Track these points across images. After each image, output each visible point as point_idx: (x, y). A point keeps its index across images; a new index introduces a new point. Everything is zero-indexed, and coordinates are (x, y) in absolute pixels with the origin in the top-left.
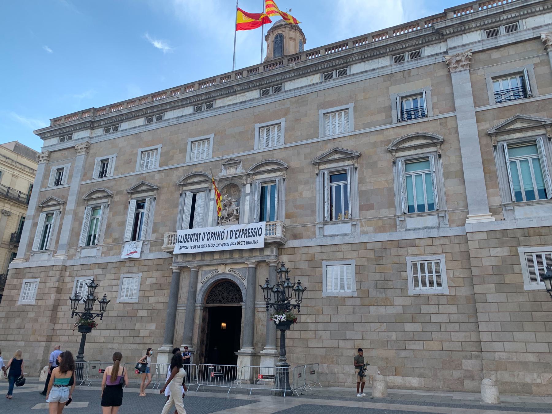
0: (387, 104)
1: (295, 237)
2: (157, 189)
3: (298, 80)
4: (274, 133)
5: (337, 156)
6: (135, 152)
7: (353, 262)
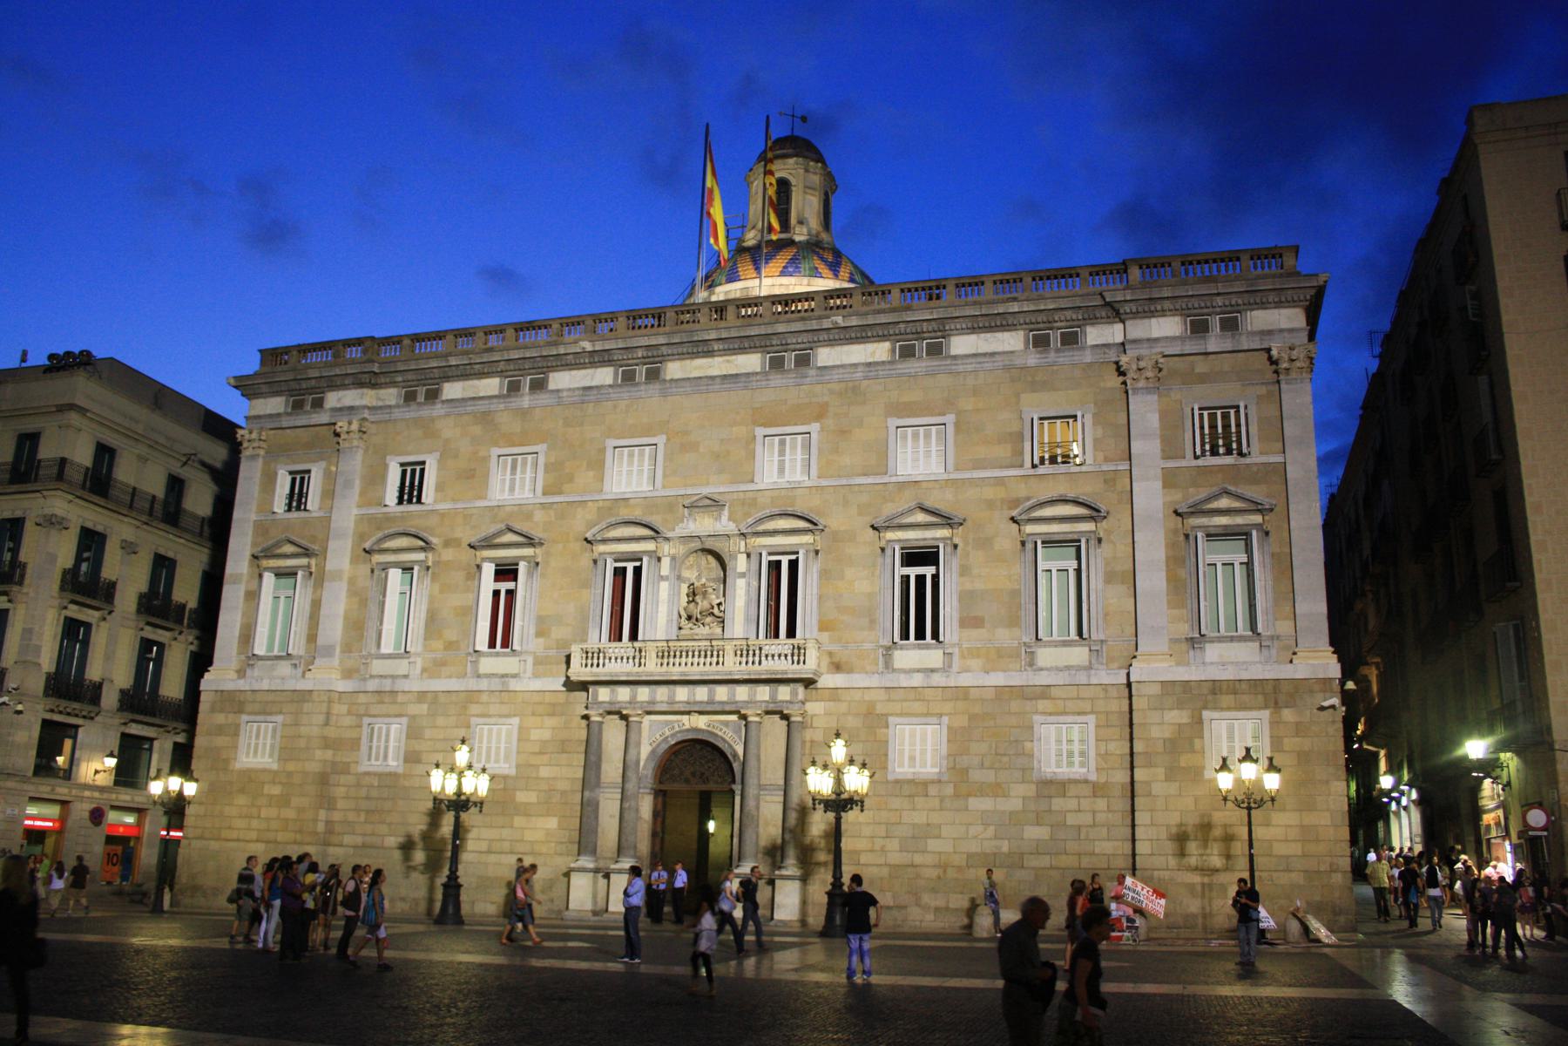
0: (1015, 428)
1: (837, 667)
3: (846, 348)
5: (921, 517)
6: (482, 454)
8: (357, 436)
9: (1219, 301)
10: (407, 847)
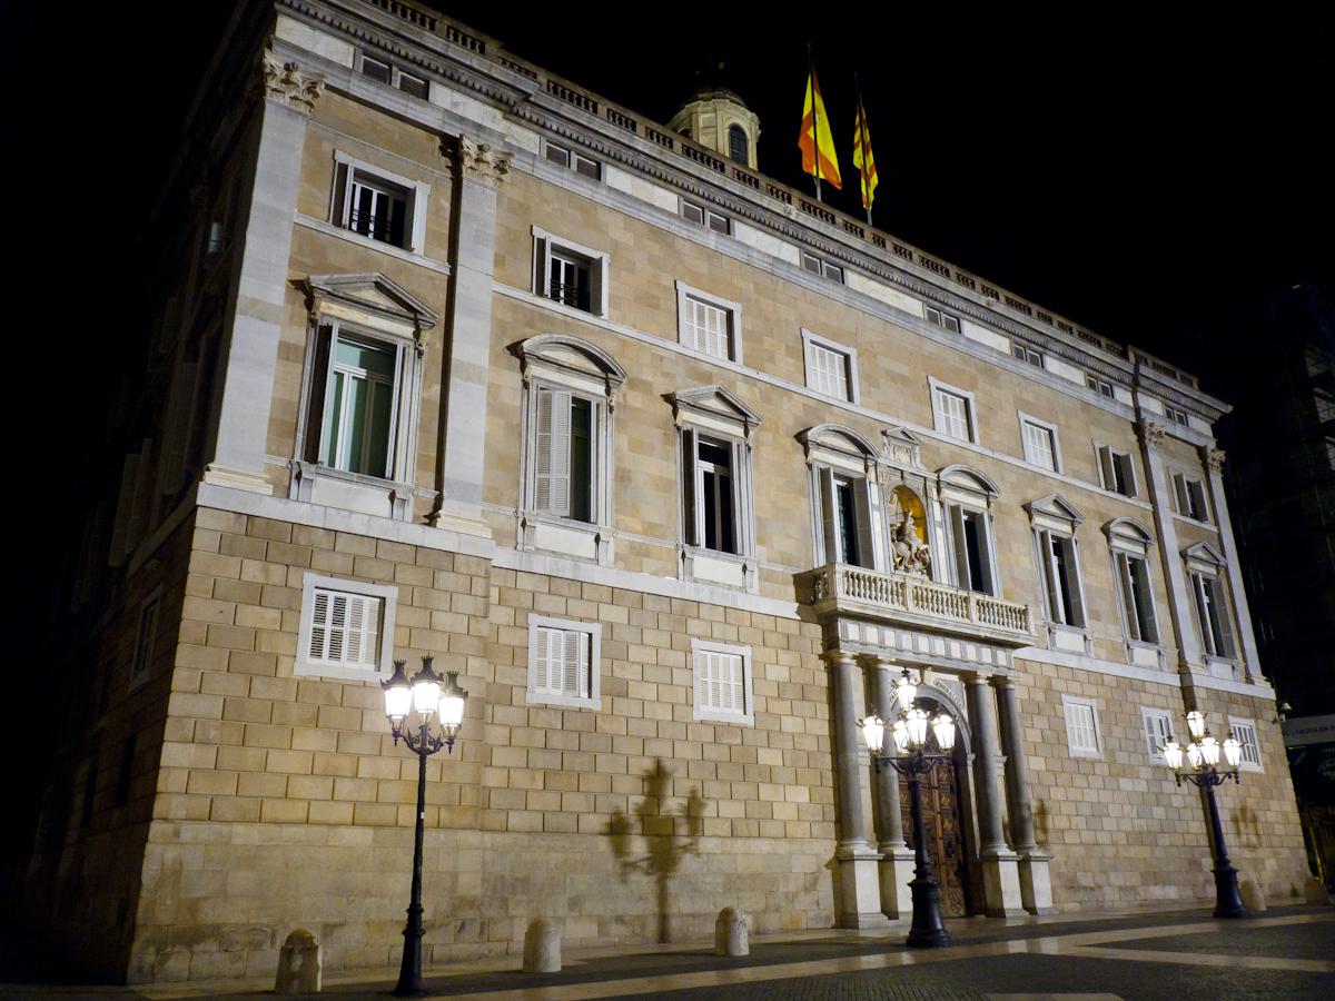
5: (1053, 509)
7: (1094, 703)
8: (491, 171)
9: (1183, 400)
10: (617, 830)
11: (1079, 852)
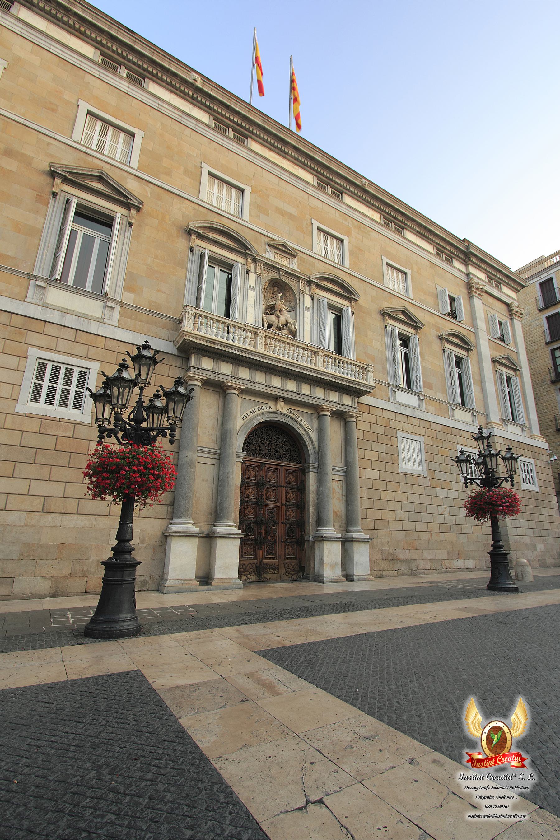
2: (138, 209)
4: (333, 247)
5: (401, 316)
7: (422, 438)
11: (401, 536)
